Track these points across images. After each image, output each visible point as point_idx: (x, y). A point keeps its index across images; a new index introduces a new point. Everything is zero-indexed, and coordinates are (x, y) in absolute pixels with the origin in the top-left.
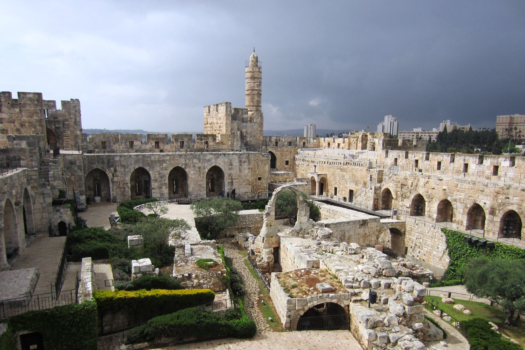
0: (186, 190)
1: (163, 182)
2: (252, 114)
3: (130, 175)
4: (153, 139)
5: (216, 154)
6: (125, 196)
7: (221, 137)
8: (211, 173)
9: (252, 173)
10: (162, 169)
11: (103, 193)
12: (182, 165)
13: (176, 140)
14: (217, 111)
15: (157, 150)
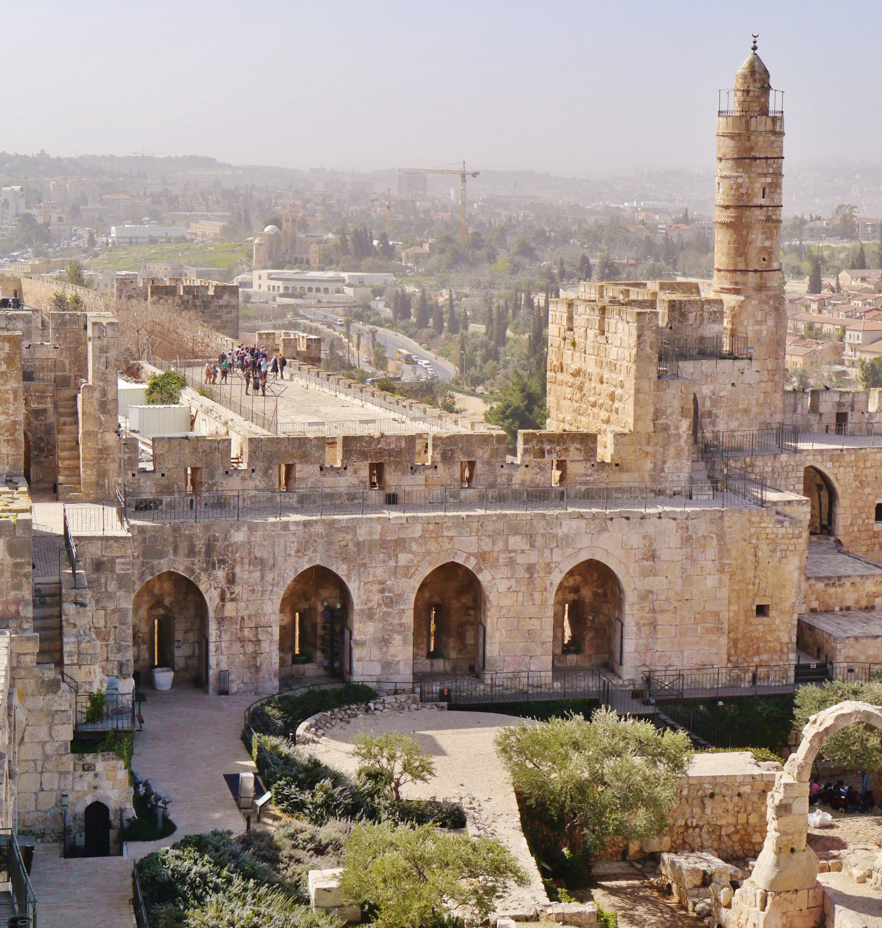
0: (476, 645)
1: (396, 621)
2: (742, 305)
3: (280, 593)
4: (364, 455)
5: (594, 516)
6: (258, 669)
7: (616, 445)
8: (571, 582)
9: (732, 590)
10: (395, 572)
11: (180, 653)
12: (467, 559)
13: (447, 457)
14: (603, 332)
15: (375, 496)
